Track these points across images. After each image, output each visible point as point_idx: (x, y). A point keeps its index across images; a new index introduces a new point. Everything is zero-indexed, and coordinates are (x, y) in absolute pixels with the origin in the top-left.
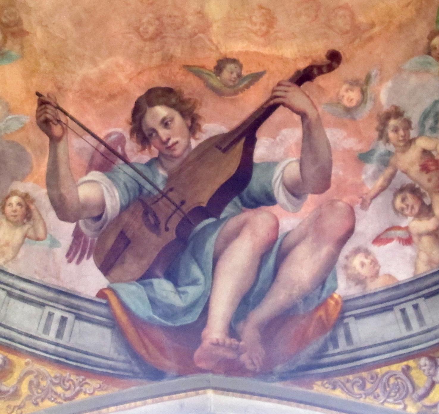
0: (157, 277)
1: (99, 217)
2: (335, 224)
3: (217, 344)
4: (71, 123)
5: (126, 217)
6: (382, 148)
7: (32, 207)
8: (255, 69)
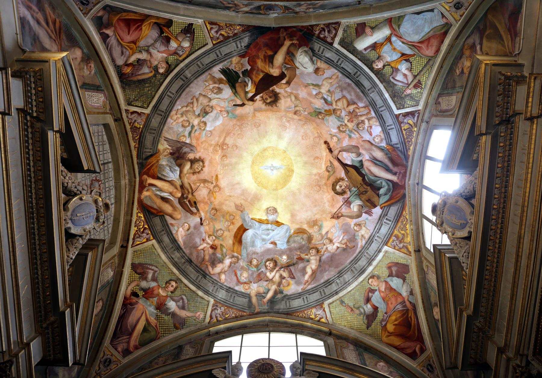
2: (367, 145)
3: (398, 178)
5: (363, 199)
6: (348, 132)
8: (329, 162)
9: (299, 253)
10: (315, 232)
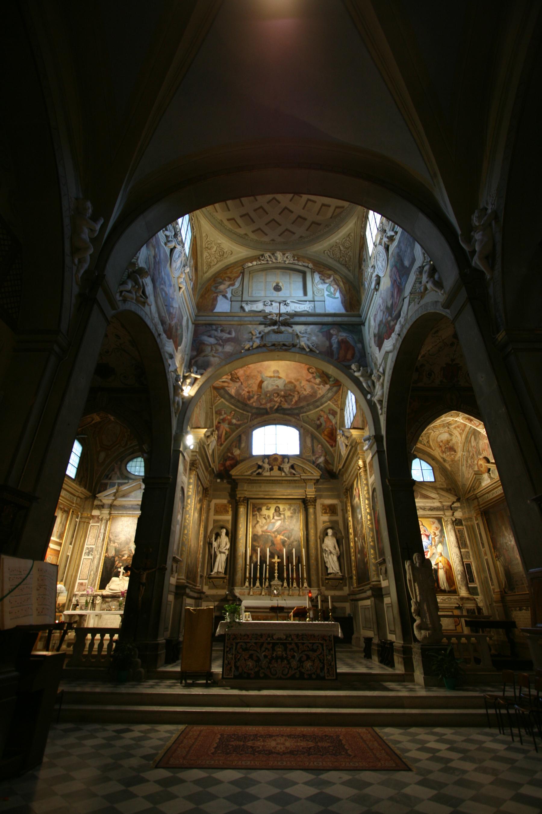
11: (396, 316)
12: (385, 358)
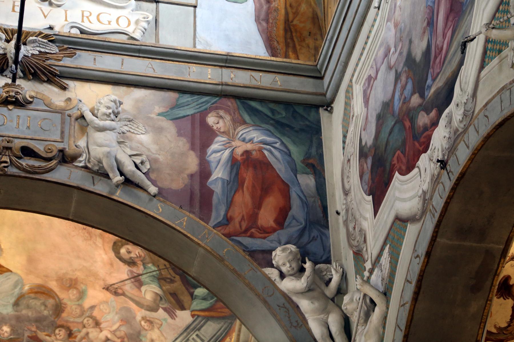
0: (194, 292)
1: (161, 298)
4: (119, 285)
7: (148, 319)
9: (34, 329)
10: (70, 300)
11: (437, 93)
12: (393, 239)
